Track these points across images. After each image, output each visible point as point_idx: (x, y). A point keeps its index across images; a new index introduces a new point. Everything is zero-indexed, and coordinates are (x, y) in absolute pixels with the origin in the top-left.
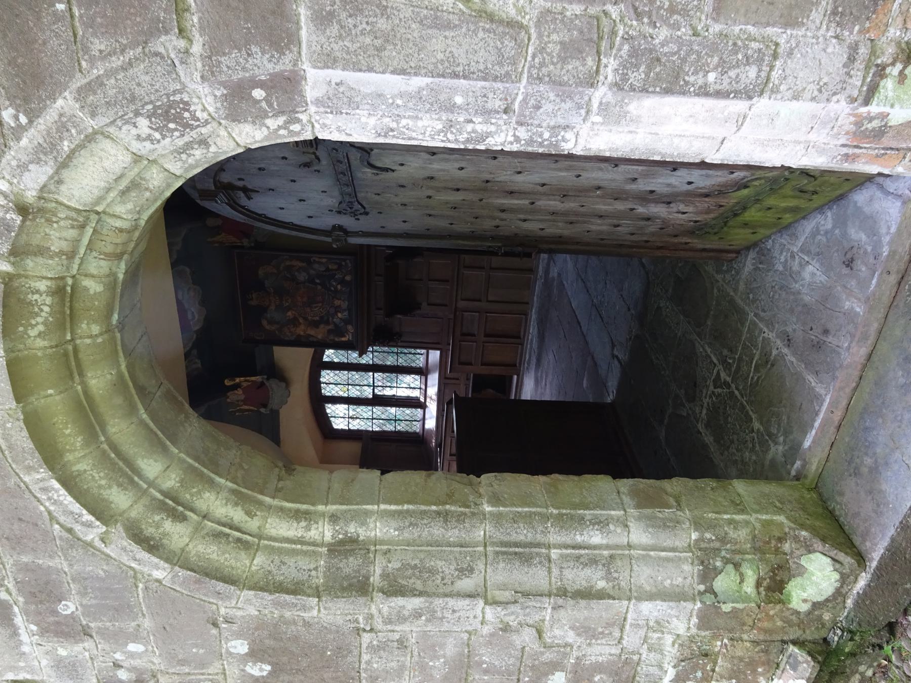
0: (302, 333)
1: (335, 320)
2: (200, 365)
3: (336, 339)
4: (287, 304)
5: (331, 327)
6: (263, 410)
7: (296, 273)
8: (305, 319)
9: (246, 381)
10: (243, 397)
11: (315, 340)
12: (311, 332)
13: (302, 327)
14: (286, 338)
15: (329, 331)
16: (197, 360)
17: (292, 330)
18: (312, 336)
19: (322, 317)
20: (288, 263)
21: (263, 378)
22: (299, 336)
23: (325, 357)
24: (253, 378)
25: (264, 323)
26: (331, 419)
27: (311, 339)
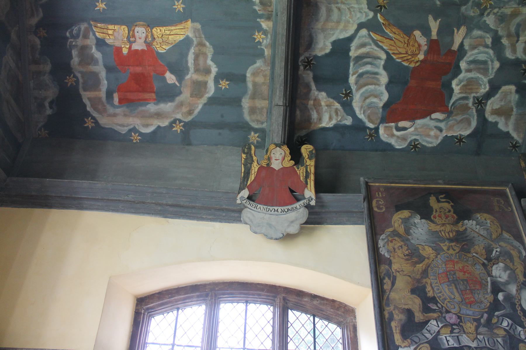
0: (395, 267)
1: (434, 322)
2: (324, 125)
3: (393, 324)
4: (445, 248)
5: (419, 317)
6: (245, 193)
7: (501, 265)
8: (425, 273)
9: (307, 176)
10: (276, 165)
11: (385, 287)
12: (401, 283)
13: (407, 267)
14: (381, 243)
15: (409, 313)
16: (334, 122)
17: (399, 253)
18: (393, 284)
19: (434, 300)
20: (514, 253)
21: (310, 199)
22: (390, 263)
23: (298, 313)
24: (311, 183)
25: (406, 213)
26: (175, 312)
27: (387, 282)
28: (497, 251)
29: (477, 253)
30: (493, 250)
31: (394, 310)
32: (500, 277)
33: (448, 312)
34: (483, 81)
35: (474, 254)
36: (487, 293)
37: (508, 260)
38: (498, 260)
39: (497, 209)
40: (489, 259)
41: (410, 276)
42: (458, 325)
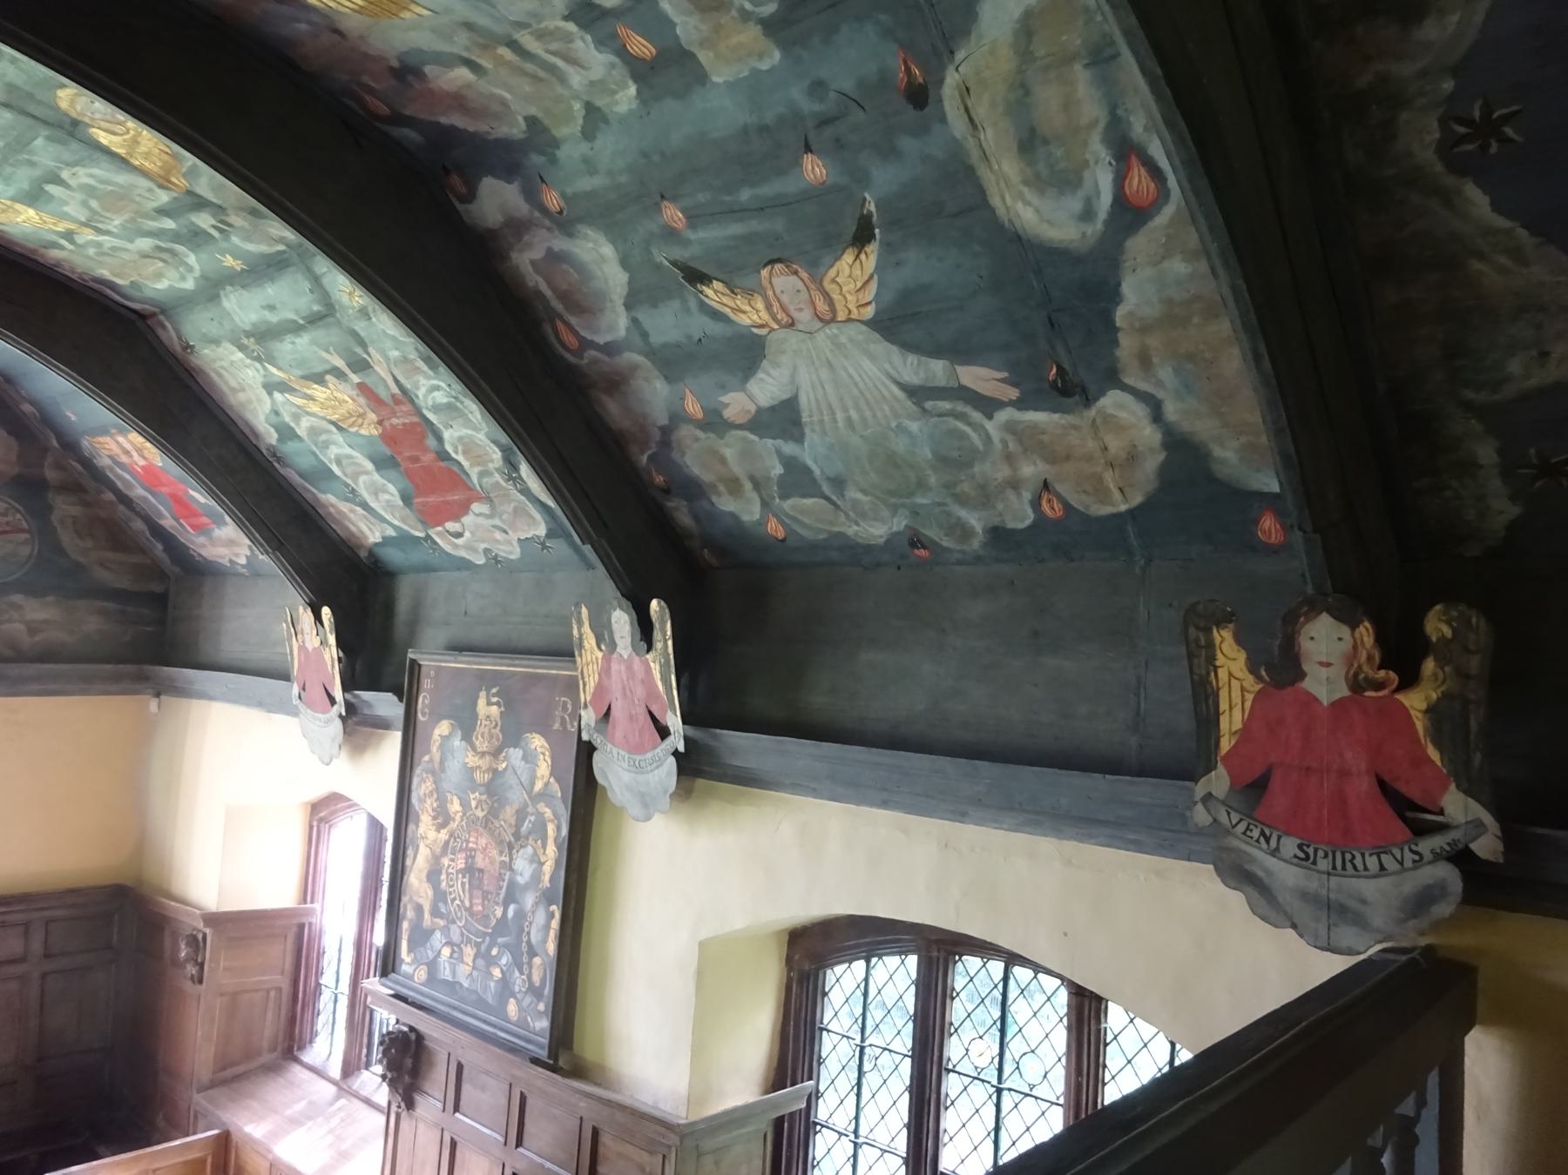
13: (432, 834)
28: (530, 821)
29: (505, 822)
30: (526, 818)
31: (409, 901)
32: (521, 875)
33: (454, 922)
34: (481, 440)
35: (502, 823)
36: (497, 904)
37: (539, 842)
38: (527, 839)
39: (557, 726)
40: (517, 835)
41: (430, 848)
42: (459, 946)
